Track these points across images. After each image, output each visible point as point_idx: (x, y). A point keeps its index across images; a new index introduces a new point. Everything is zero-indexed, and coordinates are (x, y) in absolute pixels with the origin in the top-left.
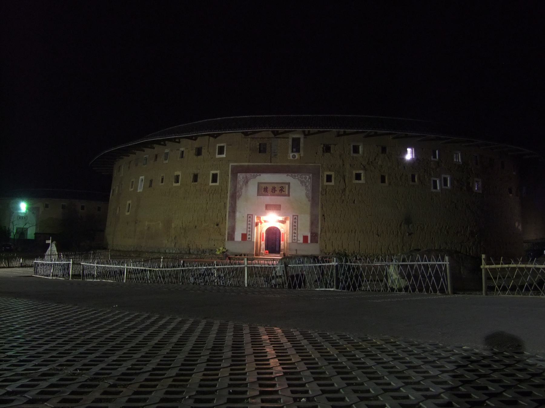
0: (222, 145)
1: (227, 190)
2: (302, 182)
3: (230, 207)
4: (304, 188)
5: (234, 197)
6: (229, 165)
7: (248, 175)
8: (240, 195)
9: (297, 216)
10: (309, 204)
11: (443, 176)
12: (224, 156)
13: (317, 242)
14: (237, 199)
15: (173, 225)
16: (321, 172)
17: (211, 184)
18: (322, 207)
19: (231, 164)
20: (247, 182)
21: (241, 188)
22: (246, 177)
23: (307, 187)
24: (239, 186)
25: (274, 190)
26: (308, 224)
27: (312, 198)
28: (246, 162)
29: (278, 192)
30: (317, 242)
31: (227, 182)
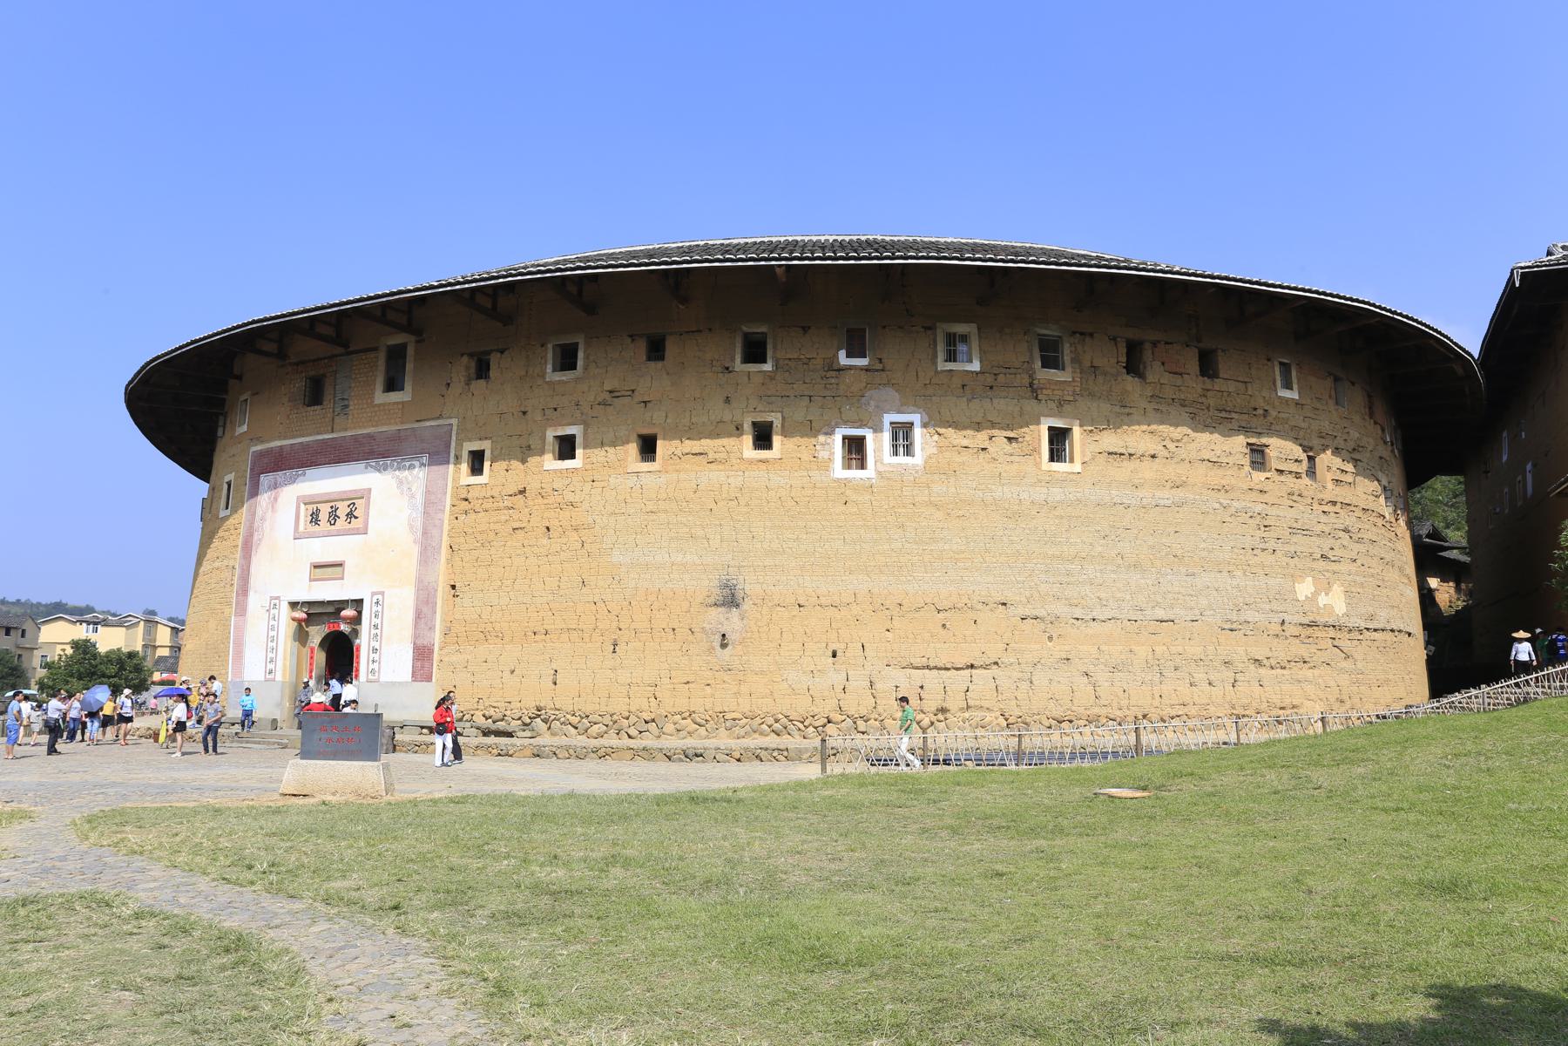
9: (383, 593)
10: (415, 550)
11: (888, 418)
13: (429, 679)
16: (453, 444)
18: (448, 561)
24: (259, 512)
25: (333, 516)
26: (410, 616)
27: (425, 533)
28: (280, 438)
30: (429, 679)
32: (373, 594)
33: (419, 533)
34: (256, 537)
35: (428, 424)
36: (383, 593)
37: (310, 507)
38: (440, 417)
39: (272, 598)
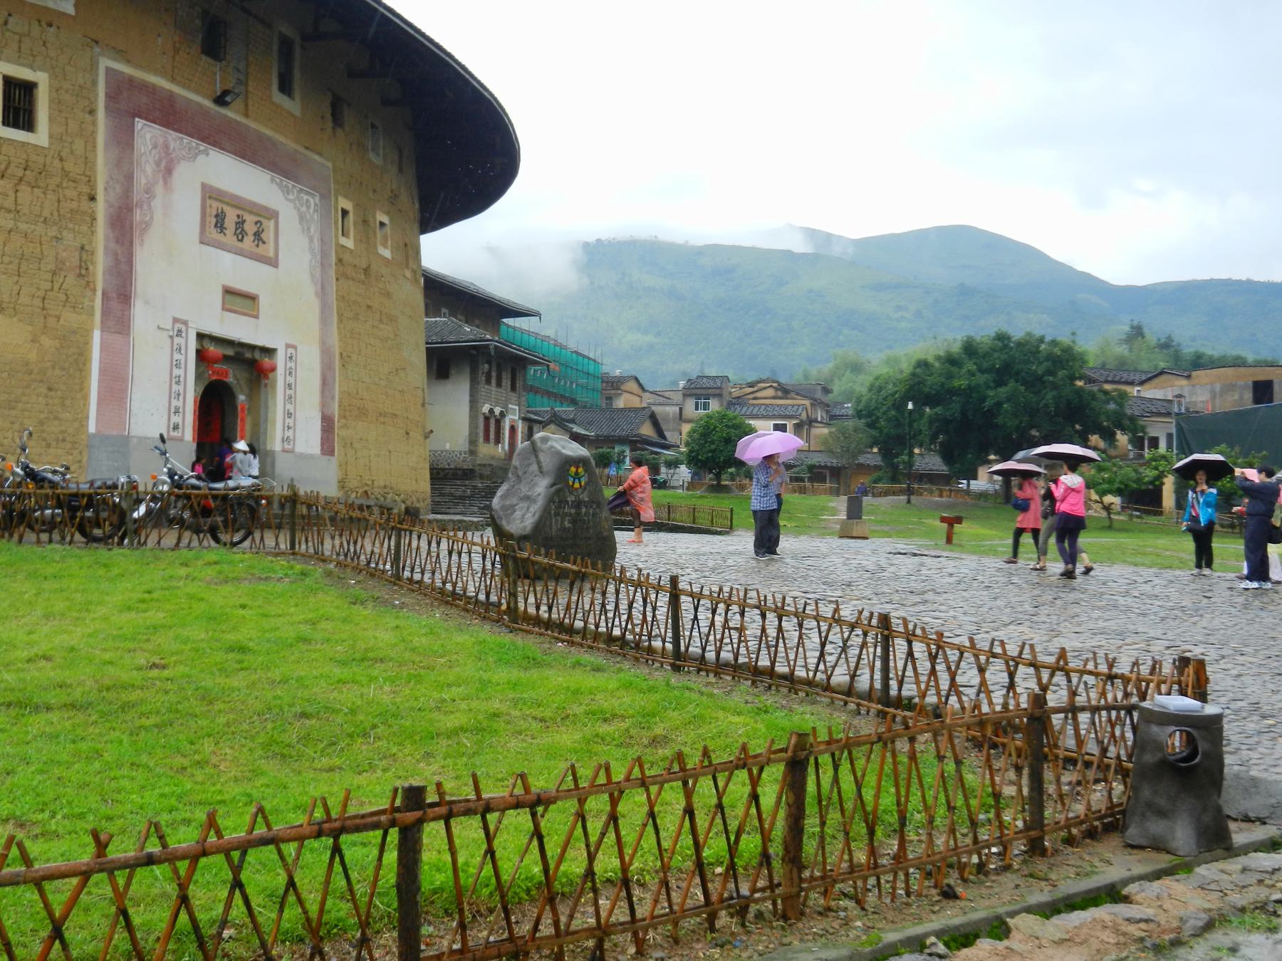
1: (91, 182)
2: (302, 218)
3: (108, 271)
4: (305, 242)
5: (125, 227)
6: (94, 66)
7: (176, 140)
8: (147, 226)
14: (136, 241)
18: (339, 328)
19: (105, 63)
20: (169, 171)
22: (166, 146)
23: (311, 239)
24: (141, 180)
28: (162, 73)
29: (249, 242)
31: (91, 141)
32: (288, 346)
33: (319, 286)
34: (138, 216)
35: (316, 157)
36: (295, 347)
37: (215, 204)
38: (320, 154)
39: (176, 320)
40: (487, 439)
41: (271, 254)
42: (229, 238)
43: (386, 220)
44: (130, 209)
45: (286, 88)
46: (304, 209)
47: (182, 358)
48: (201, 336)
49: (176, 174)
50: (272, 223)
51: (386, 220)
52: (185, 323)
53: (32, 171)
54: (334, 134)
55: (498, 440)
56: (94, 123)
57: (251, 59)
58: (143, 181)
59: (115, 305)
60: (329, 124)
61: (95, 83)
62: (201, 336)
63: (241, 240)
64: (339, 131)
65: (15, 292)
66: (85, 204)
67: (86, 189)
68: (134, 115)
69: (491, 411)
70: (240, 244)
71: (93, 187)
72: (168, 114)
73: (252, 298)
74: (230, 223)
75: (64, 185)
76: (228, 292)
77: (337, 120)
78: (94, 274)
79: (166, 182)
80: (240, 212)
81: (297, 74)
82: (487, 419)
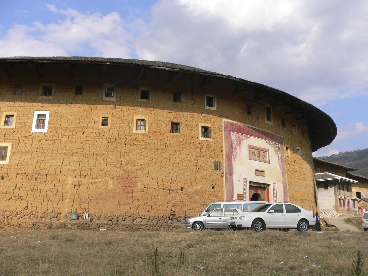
0: (211, 96)
1: (222, 147)
2: (275, 151)
4: (277, 157)
5: (230, 158)
8: (236, 156)
9: (276, 183)
10: (281, 172)
12: (215, 108)
14: (233, 160)
15: (139, 185)
17: (201, 138)
19: (224, 120)
20: (240, 143)
21: (236, 148)
29: (261, 158)
32: (274, 183)
35: (278, 135)
36: (276, 183)
37: (252, 149)
38: (279, 134)
39: (243, 179)
40: (341, 206)
41: (268, 160)
42: (256, 157)
43: (299, 148)
44: (231, 153)
45: (269, 119)
46: (276, 148)
47: (246, 188)
48: (250, 182)
49: (242, 143)
50: (267, 152)
51: (299, 148)
52: (246, 179)
53: (208, 147)
54: (283, 129)
55: (344, 206)
56: (222, 134)
57: (259, 114)
58: (234, 146)
59: (229, 176)
60: (281, 126)
61: (222, 125)
62: (250, 182)
63: (260, 158)
64: (284, 128)
65: (206, 175)
66: (220, 153)
67: (221, 149)
68: (231, 131)
69: (341, 197)
70: (259, 159)
71: (222, 149)
72: (239, 130)
73: (263, 172)
74: (256, 153)
75: (216, 149)
76: (257, 170)
77: (284, 125)
78: (223, 169)
79: (239, 145)
80: (259, 151)
81: (272, 115)
82: (340, 200)
